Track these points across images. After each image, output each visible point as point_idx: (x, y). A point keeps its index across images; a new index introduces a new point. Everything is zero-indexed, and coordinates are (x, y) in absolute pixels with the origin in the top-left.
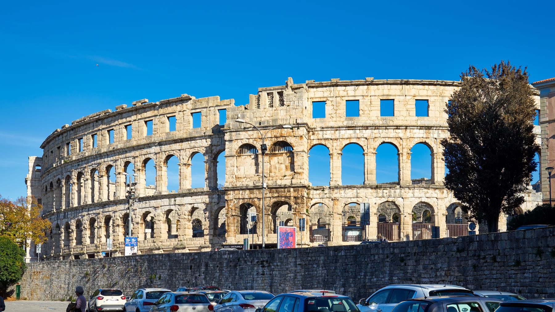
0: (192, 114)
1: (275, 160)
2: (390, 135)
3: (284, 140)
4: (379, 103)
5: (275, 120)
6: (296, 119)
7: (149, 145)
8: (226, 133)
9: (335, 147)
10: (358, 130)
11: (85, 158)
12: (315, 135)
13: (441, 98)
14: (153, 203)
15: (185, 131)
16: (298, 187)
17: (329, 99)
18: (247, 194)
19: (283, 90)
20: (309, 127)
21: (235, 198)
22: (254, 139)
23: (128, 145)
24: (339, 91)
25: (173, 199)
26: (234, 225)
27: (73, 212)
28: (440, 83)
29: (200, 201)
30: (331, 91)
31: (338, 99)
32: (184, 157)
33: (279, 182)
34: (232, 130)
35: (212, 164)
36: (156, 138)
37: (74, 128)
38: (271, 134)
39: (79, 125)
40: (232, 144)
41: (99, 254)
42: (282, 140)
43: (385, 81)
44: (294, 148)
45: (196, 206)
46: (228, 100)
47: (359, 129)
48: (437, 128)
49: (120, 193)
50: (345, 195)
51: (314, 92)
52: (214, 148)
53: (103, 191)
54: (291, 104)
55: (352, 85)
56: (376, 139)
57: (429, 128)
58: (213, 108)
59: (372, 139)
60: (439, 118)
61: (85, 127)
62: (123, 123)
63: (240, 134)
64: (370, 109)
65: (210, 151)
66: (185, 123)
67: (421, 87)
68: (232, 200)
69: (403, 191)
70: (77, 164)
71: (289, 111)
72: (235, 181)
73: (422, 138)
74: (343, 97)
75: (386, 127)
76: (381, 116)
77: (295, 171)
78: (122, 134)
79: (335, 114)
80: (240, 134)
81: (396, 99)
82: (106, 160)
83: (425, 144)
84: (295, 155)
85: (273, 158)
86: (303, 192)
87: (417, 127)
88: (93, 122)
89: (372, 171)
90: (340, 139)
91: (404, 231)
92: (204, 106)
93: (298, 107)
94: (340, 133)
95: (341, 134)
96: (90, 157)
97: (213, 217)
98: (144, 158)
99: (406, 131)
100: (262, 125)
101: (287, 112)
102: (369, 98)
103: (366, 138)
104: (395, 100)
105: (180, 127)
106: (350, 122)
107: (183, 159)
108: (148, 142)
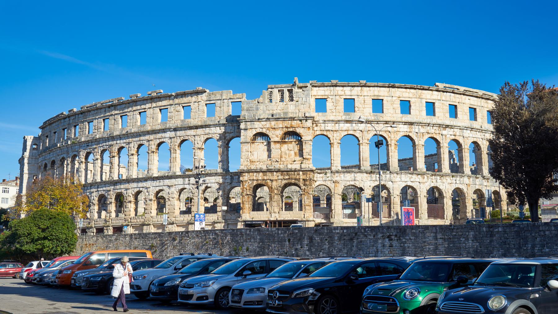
0: (206, 104)
1: (285, 147)
2: (381, 128)
4: (371, 101)
5: (286, 113)
6: (305, 113)
7: (164, 131)
8: (242, 122)
9: (336, 138)
10: (355, 124)
11: (96, 139)
12: (318, 126)
13: (420, 100)
14: (167, 182)
15: (200, 119)
16: (306, 171)
17: (329, 97)
18: (260, 176)
19: (292, 88)
21: (250, 179)
22: (267, 129)
23: (142, 129)
24: (338, 90)
25: (187, 179)
26: (249, 203)
28: (419, 87)
29: (214, 181)
31: (337, 97)
32: (199, 142)
33: (290, 166)
35: (225, 149)
36: (171, 124)
37: (84, 112)
39: (91, 110)
41: (109, 228)
43: (376, 84)
44: (303, 138)
46: (240, 94)
47: (356, 123)
48: (418, 124)
49: (132, 173)
50: (345, 179)
52: (227, 135)
53: (114, 170)
54: (300, 100)
55: (349, 86)
57: (411, 124)
58: (227, 100)
59: (366, 131)
60: (418, 116)
61: (96, 111)
62: (137, 110)
63: (254, 124)
64: (364, 107)
65: (224, 138)
66: (199, 113)
67: (404, 90)
68: (247, 181)
69: (392, 176)
70: (85, 145)
71: (298, 106)
72: (250, 164)
74: (341, 95)
75: (377, 122)
76: (373, 112)
77: (304, 157)
78: (136, 120)
79: (335, 110)
80: (254, 124)
81: (385, 99)
82: (118, 142)
84: (304, 144)
87: (402, 122)
88: (105, 108)
89: (366, 159)
91: (394, 210)
92: (218, 98)
94: (339, 126)
95: (340, 127)
96: (102, 139)
97: (225, 195)
98: (158, 141)
100: (274, 117)
101: (296, 107)
102: (363, 97)
103: (361, 131)
105: (195, 116)
106: (348, 117)
107: (198, 144)
108: (163, 127)
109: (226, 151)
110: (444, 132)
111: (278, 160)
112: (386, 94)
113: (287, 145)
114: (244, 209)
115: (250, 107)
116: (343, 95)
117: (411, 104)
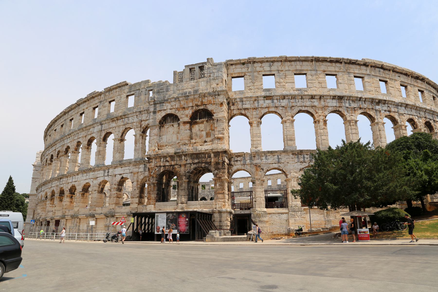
1: (196, 128)
3: (204, 108)
15: (120, 111)
17: (246, 74)
20: (229, 98)
22: (176, 109)
30: (248, 68)
31: (256, 74)
34: (157, 102)
35: (141, 137)
38: (193, 103)
40: (156, 115)
42: (202, 108)
45: (124, 176)
47: (277, 100)
51: (233, 69)
52: (143, 122)
55: (267, 61)
56: (293, 107)
57: (340, 98)
59: (289, 107)
63: (163, 105)
65: (140, 126)
67: (329, 64)
68: (153, 168)
71: (210, 82)
73: (335, 107)
80: (163, 105)
81: (309, 73)
83: (338, 114)
85: (194, 126)
86: (224, 158)
90: (259, 108)
93: (217, 78)
95: (259, 104)
96: (57, 142)
97: (139, 186)
98: (89, 137)
99: (320, 100)
101: (207, 83)
104: (307, 74)
106: (268, 93)
109: (141, 140)
110: (378, 107)
111: (187, 142)
112: (309, 68)
113: (198, 125)
114: (150, 199)
115: (161, 89)
116: (261, 71)
117: (339, 78)
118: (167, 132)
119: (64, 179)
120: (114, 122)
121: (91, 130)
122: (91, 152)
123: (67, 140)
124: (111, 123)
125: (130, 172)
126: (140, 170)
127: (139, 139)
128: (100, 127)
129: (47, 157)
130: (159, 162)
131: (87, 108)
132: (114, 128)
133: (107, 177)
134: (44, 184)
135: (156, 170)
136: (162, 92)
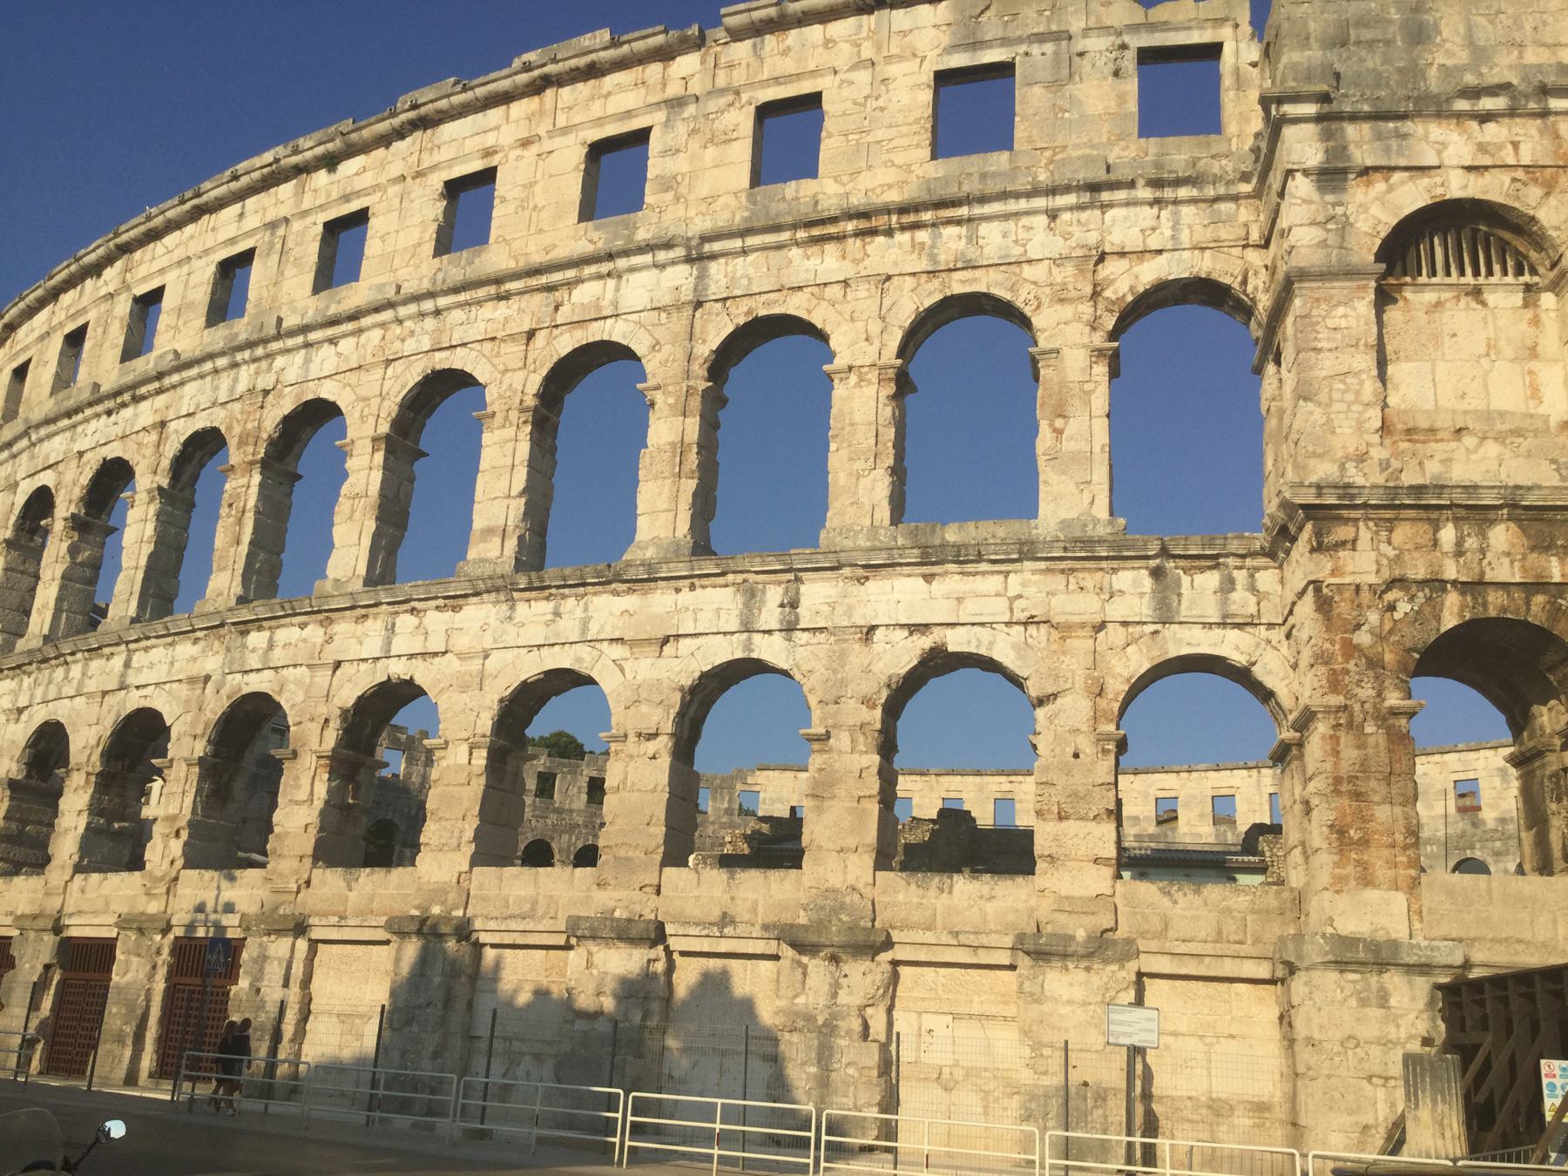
15: (891, 176)
22: (1520, 174)
27: (27, 681)
29: (997, 609)
35: (1101, 370)
40: (1345, 198)
45: (957, 642)
52: (1111, 268)
63: (1405, 136)
65: (1088, 290)
80: (1405, 136)
92: (1041, 29)
96: (194, 372)
114: (1364, 843)
115: (1362, 23)
118: (1436, 338)
119: (288, 634)
120: (830, 248)
121: (586, 293)
122: (558, 457)
123: (307, 360)
124: (795, 252)
125: (1020, 616)
126: (1116, 611)
127: (1087, 387)
128: (681, 277)
129: (47, 479)
130: (1418, 547)
131: (525, 143)
132: (835, 291)
133: (778, 637)
134: (19, 667)
135: (1392, 608)
136: (1370, 44)
